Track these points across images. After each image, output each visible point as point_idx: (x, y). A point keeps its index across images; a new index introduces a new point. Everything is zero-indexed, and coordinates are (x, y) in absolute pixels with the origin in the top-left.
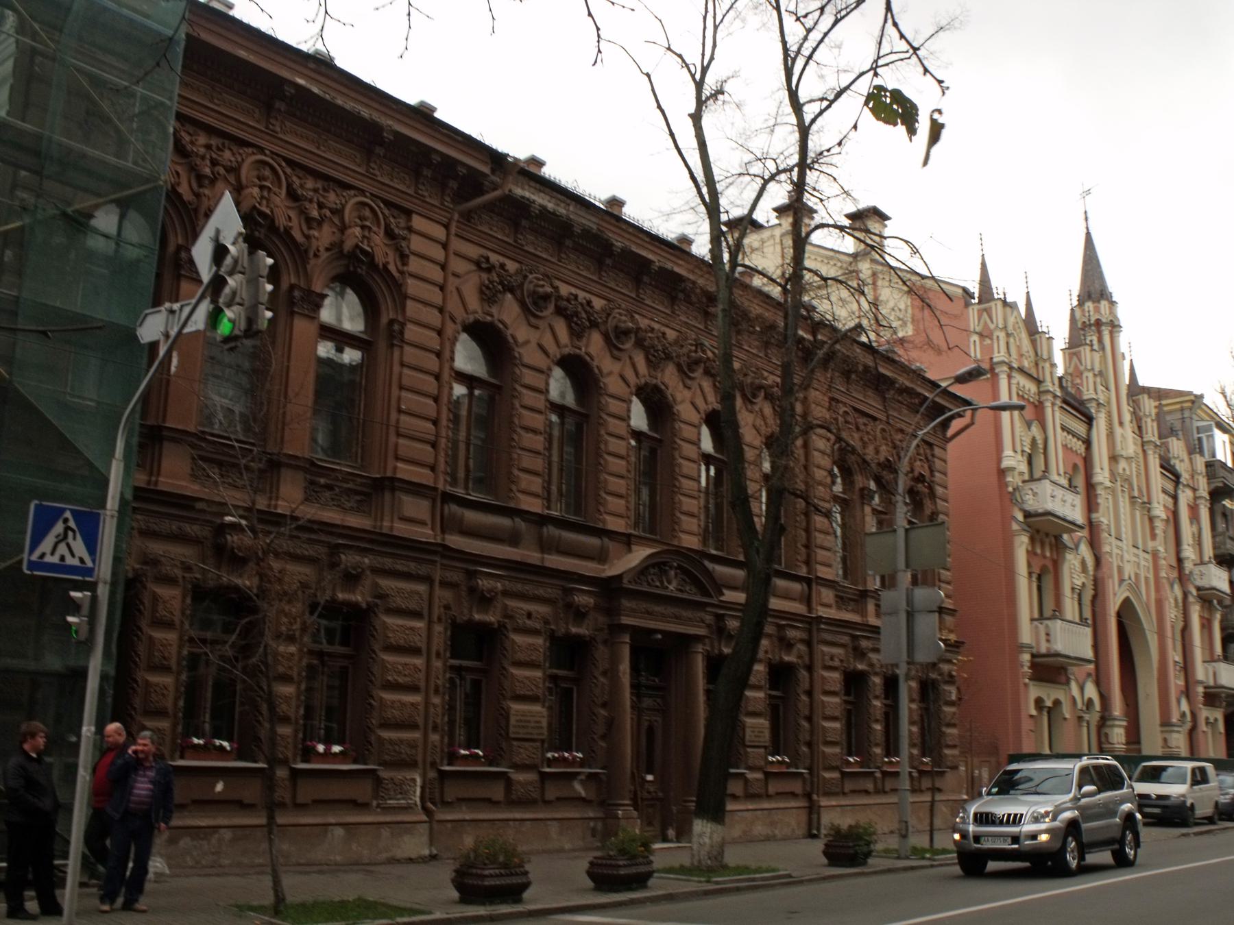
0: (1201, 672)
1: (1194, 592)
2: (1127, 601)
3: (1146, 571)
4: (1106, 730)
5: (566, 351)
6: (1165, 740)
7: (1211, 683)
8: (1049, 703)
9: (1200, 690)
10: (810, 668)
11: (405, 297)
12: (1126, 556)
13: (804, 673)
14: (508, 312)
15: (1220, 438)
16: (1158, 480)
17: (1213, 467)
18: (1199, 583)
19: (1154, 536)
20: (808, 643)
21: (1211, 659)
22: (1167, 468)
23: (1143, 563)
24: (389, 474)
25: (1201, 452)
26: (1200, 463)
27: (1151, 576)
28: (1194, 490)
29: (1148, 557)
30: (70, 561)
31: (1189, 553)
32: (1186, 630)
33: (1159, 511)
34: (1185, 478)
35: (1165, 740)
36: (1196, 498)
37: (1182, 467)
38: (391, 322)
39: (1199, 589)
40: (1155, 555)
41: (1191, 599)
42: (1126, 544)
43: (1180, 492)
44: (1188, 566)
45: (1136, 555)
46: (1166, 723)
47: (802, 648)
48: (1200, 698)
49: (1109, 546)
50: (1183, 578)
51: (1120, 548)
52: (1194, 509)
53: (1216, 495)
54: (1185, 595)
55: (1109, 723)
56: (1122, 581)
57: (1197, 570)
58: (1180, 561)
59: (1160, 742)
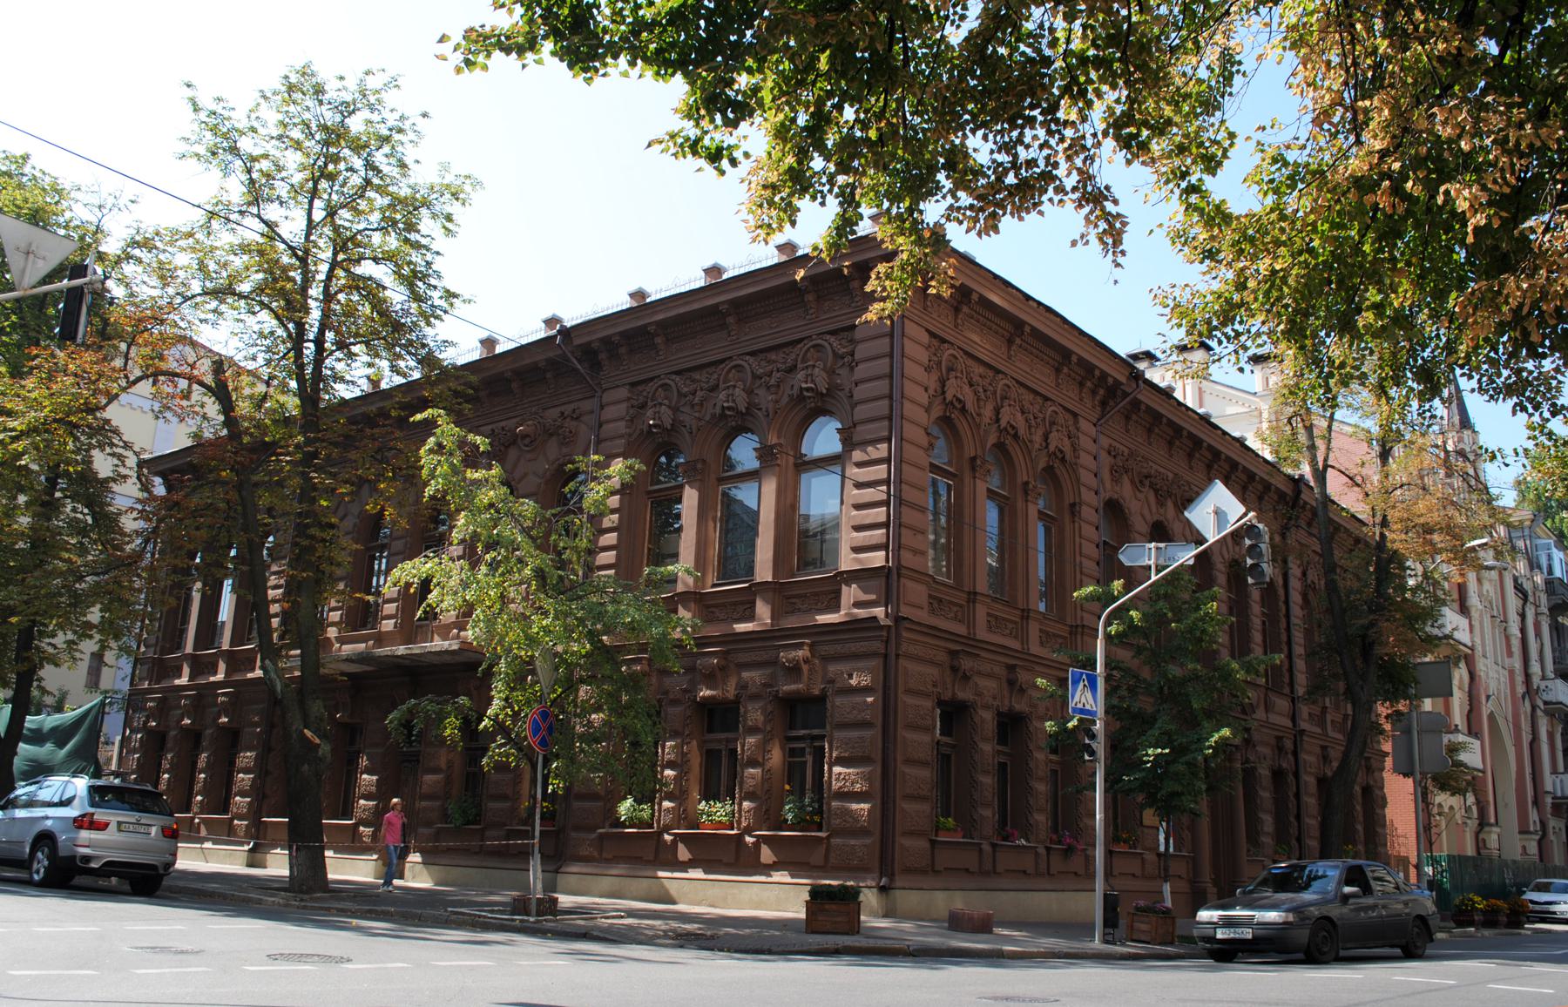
0: (1549, 782)
1: (1542, 707)
2: (1492, 712)
3: (1505, 689)
4: (1481, 836)
5: (1155, 518)
6: (1524, 848)
7: (1559, 794)
8: (1446, 810)
9: (1549, 800)
10: (1296, 775)
11: (1078, 480)
12: (1491, 674)
13: (1291, 778)
14: (1126, 491)
15: (1558, 555)
16: (1513, 602)
17: (1551, 584)
18: (1546, 697)
19: (1510, 654)
20: (1295, 753)
21: (1554, 771)
22: (1518, 587)
23: (1502, 679)
24: (1079, 623)
25: (1539, 567)
26: (1539, 579)
27: (1508, 691)
28: (1537, 606)
29: (1506, 673)
30: (1088, 707)
31: (1535, 668)
32: (1534, 741)
33: (1515, 630)
34: (1531, 599)
35: (1524, 848)
36: (1537, 614)
37: (1527, 586)
38: (1073, 505)
39: (1546, 703)
40: (1511, 672)
41: (1539, 713)
42: (1490, 662)
43: (1527, 609)
44: (1536, 681)
45: (1498, 672)
46: (1524, 831)
47: (1290, 757)
48: (1549, 809)
49: (1482, 666)
50: (1530, 691)
51: (1486, 666)
52: (1537, 625)
53: (1555, 610)
54: (1534, 708)
55: (1486, 829)
56: (1488, 697)
57: (1543, 684)
58: (1528, 677)
59: (1520, 850)
